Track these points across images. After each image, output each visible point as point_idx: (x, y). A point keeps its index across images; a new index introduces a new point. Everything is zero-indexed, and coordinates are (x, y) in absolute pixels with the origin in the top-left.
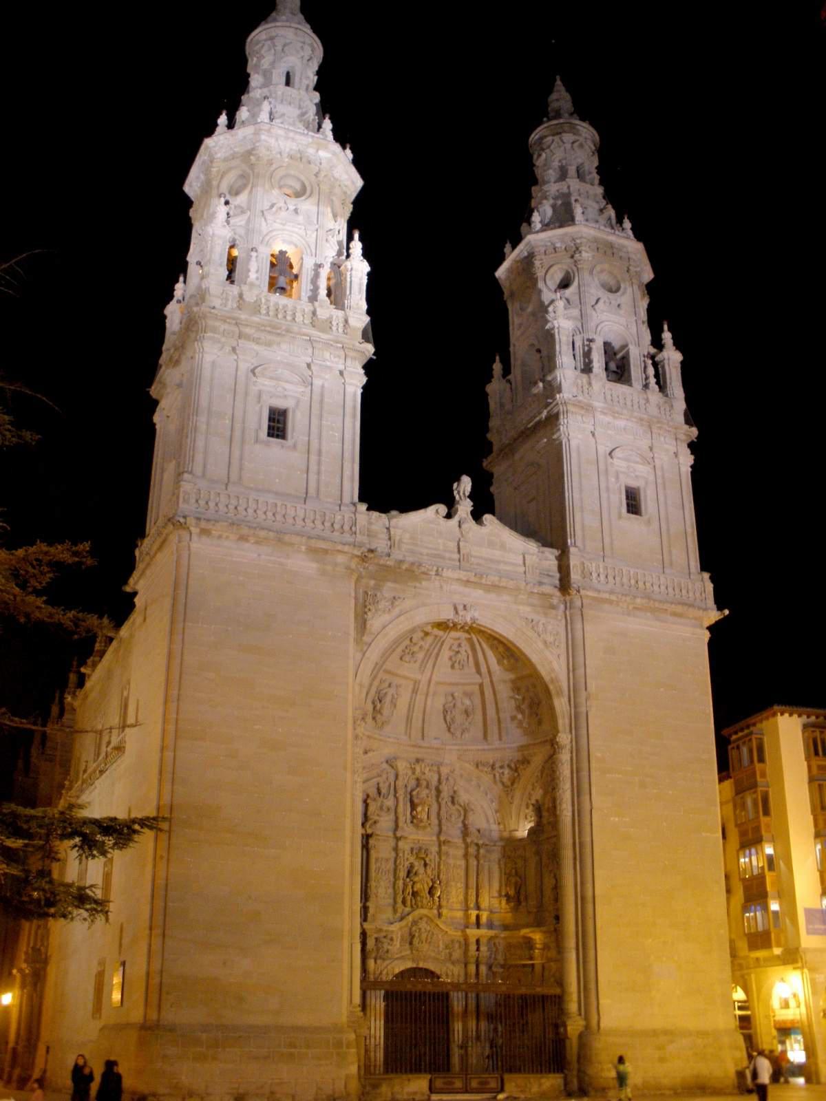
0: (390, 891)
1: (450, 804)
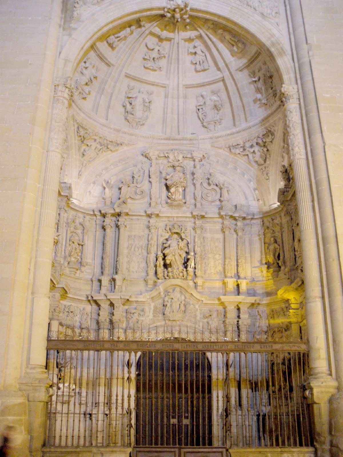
0: (143, 265)
1: (205, 185)
